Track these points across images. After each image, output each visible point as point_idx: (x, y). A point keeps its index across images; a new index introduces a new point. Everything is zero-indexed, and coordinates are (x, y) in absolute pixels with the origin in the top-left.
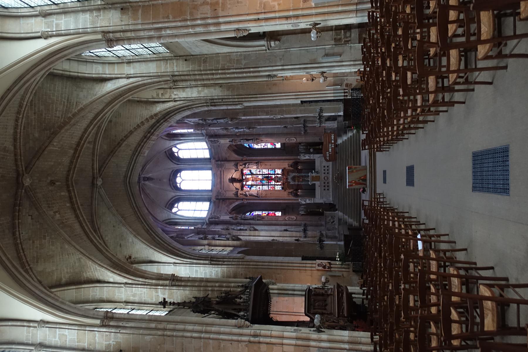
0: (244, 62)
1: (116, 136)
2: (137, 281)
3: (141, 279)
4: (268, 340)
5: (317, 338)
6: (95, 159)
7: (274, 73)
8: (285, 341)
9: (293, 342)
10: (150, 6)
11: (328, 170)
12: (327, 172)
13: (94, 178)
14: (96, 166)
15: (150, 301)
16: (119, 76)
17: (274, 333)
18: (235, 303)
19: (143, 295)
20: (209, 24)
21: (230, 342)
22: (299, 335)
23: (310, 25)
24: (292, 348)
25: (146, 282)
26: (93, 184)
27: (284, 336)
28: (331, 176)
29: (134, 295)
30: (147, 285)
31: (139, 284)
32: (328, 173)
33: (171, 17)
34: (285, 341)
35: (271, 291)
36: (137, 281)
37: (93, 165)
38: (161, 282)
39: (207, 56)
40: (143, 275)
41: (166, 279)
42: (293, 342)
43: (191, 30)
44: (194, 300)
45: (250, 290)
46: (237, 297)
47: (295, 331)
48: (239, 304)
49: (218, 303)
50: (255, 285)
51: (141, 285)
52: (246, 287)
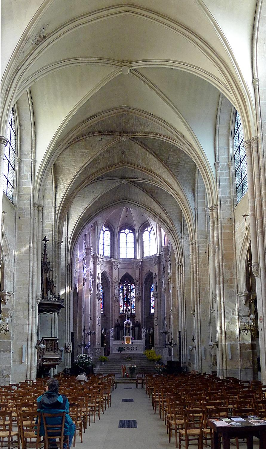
0: (203, 293)
1: (157, 193)
2: (57, 216)
3: (58, 218)
4: (30, 316)
5: (32, 346)
6: (141, 180)
7: (196, 315)
8: (30, 326)
9: (30, 331)
10: (232, 238)
11: (134, 350)
12: (133, 349)
13: (127, 178)
14: (136, 180)
15: (44, 226)
16: (196, 203)
17: (34, 319)
18: (47, 290)
19: (48, 220)
20: (219, 277)
21: (28, 291)
22: (34, 335)
23: (217, 341)
24: (26, 330)
25: (57, 222)
26: (123, 177)
27: (33, 326)
28: (130, 352)
29: (48, 214)
30: (55, 224)
31: (55, 217)
32: (132, 350)
33: (225, 252)
34: (30, 326)
35: (53, 314)
36: (57, 216)
37: (137, 178)
38: (57, 234)
39: (208, 268)
40: (61, 220)
41: (59, 238)
42: (30, 331)
43: (217, 265)
44: (48, 261)
45: (57, 301)
46: (51, 291)
47: (36, 332)
48: (47, 293)
49: (47, 279)
50: (60, 304)
51: (55, 219)
52: (58, 299)
